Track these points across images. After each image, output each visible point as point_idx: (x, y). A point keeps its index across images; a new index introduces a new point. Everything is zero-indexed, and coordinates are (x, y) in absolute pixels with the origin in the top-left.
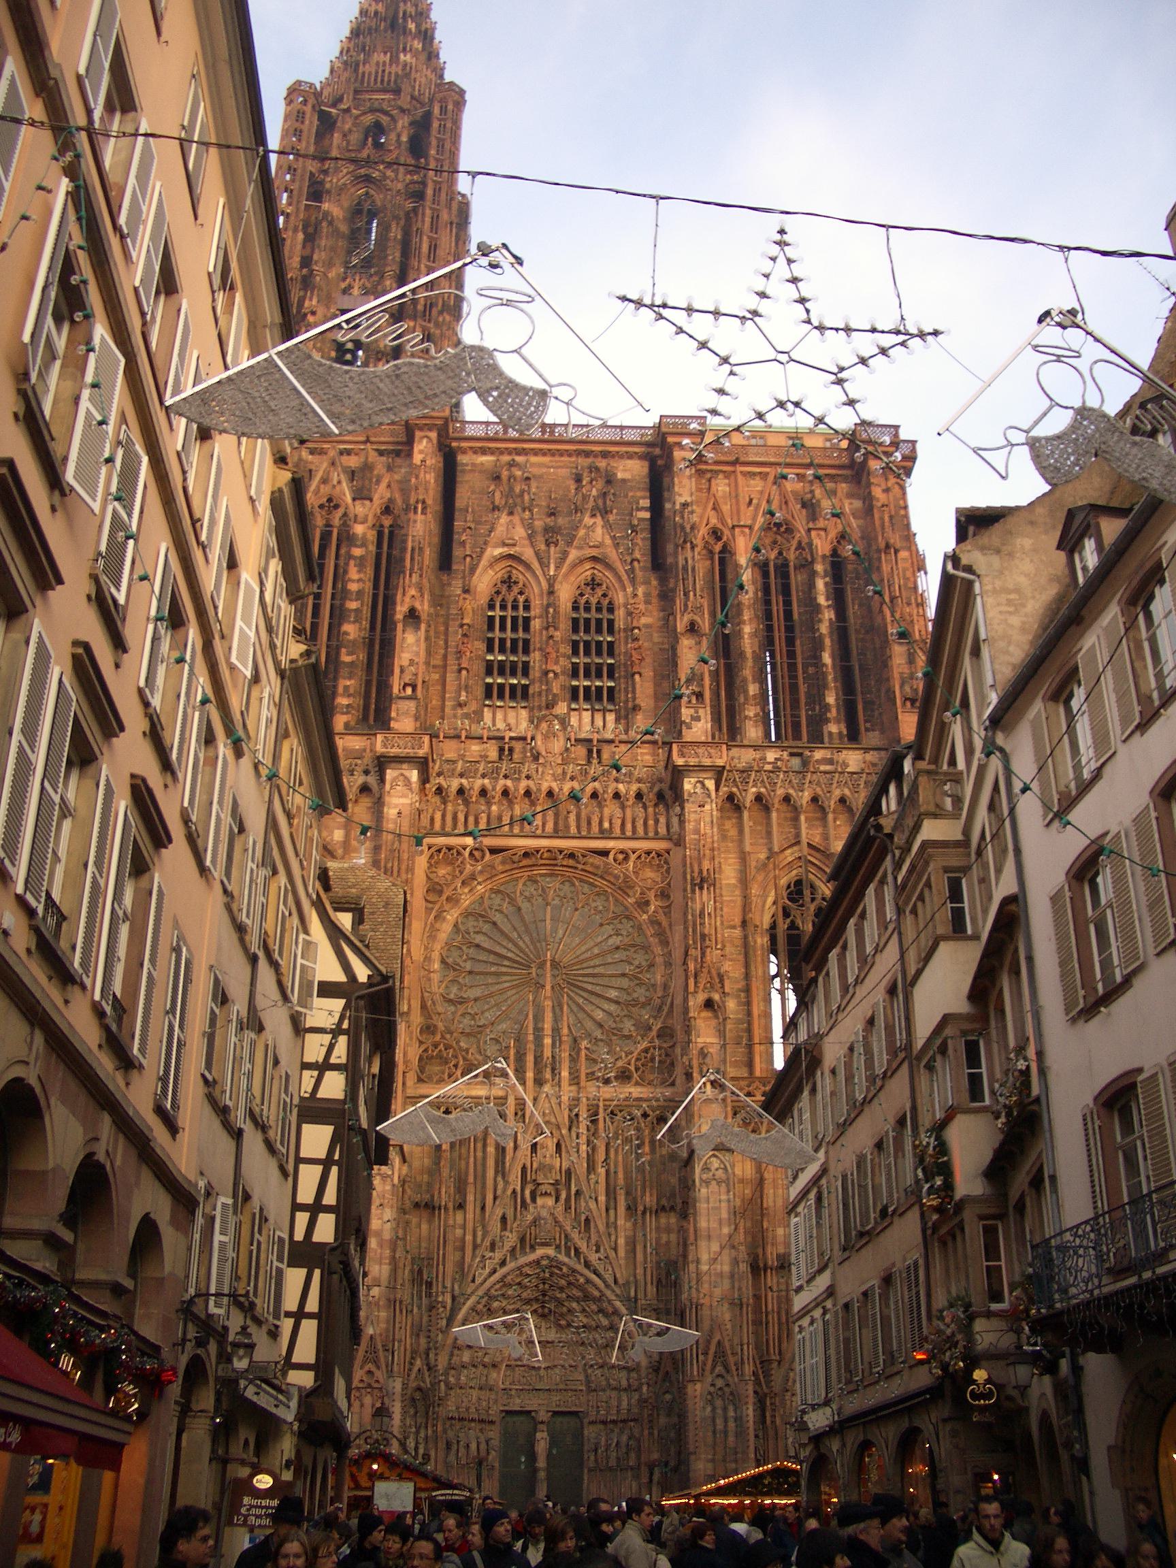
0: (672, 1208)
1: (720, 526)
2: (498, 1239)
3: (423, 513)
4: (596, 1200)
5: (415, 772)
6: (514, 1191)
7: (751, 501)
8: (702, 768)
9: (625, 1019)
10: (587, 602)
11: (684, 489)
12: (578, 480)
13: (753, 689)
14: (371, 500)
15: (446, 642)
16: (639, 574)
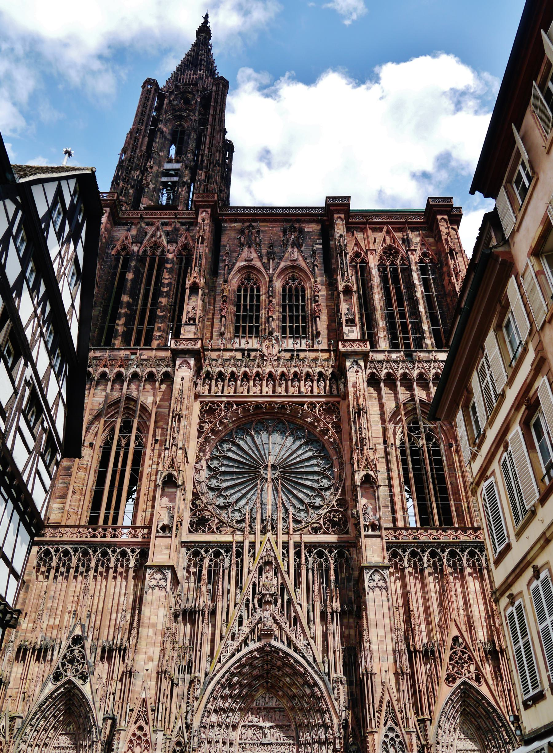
0: (350, 612)
1: (359, 251)
2: (236, 632)
3: (202, 243)
4: (301, 605)
5: (193, 359)
6: (248, 600)
7: (375, 239)
8: (355, 353)
9: (317, 499)
10: (290, 287)
11: (340, 229)
12: (284, 232)
13: (382, 324)
14: (177, 243)
15: (214, 307)
16: (317, 272)
